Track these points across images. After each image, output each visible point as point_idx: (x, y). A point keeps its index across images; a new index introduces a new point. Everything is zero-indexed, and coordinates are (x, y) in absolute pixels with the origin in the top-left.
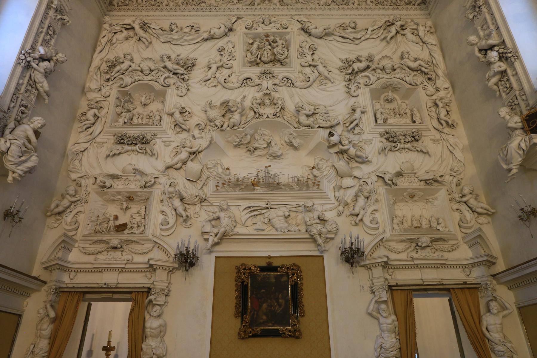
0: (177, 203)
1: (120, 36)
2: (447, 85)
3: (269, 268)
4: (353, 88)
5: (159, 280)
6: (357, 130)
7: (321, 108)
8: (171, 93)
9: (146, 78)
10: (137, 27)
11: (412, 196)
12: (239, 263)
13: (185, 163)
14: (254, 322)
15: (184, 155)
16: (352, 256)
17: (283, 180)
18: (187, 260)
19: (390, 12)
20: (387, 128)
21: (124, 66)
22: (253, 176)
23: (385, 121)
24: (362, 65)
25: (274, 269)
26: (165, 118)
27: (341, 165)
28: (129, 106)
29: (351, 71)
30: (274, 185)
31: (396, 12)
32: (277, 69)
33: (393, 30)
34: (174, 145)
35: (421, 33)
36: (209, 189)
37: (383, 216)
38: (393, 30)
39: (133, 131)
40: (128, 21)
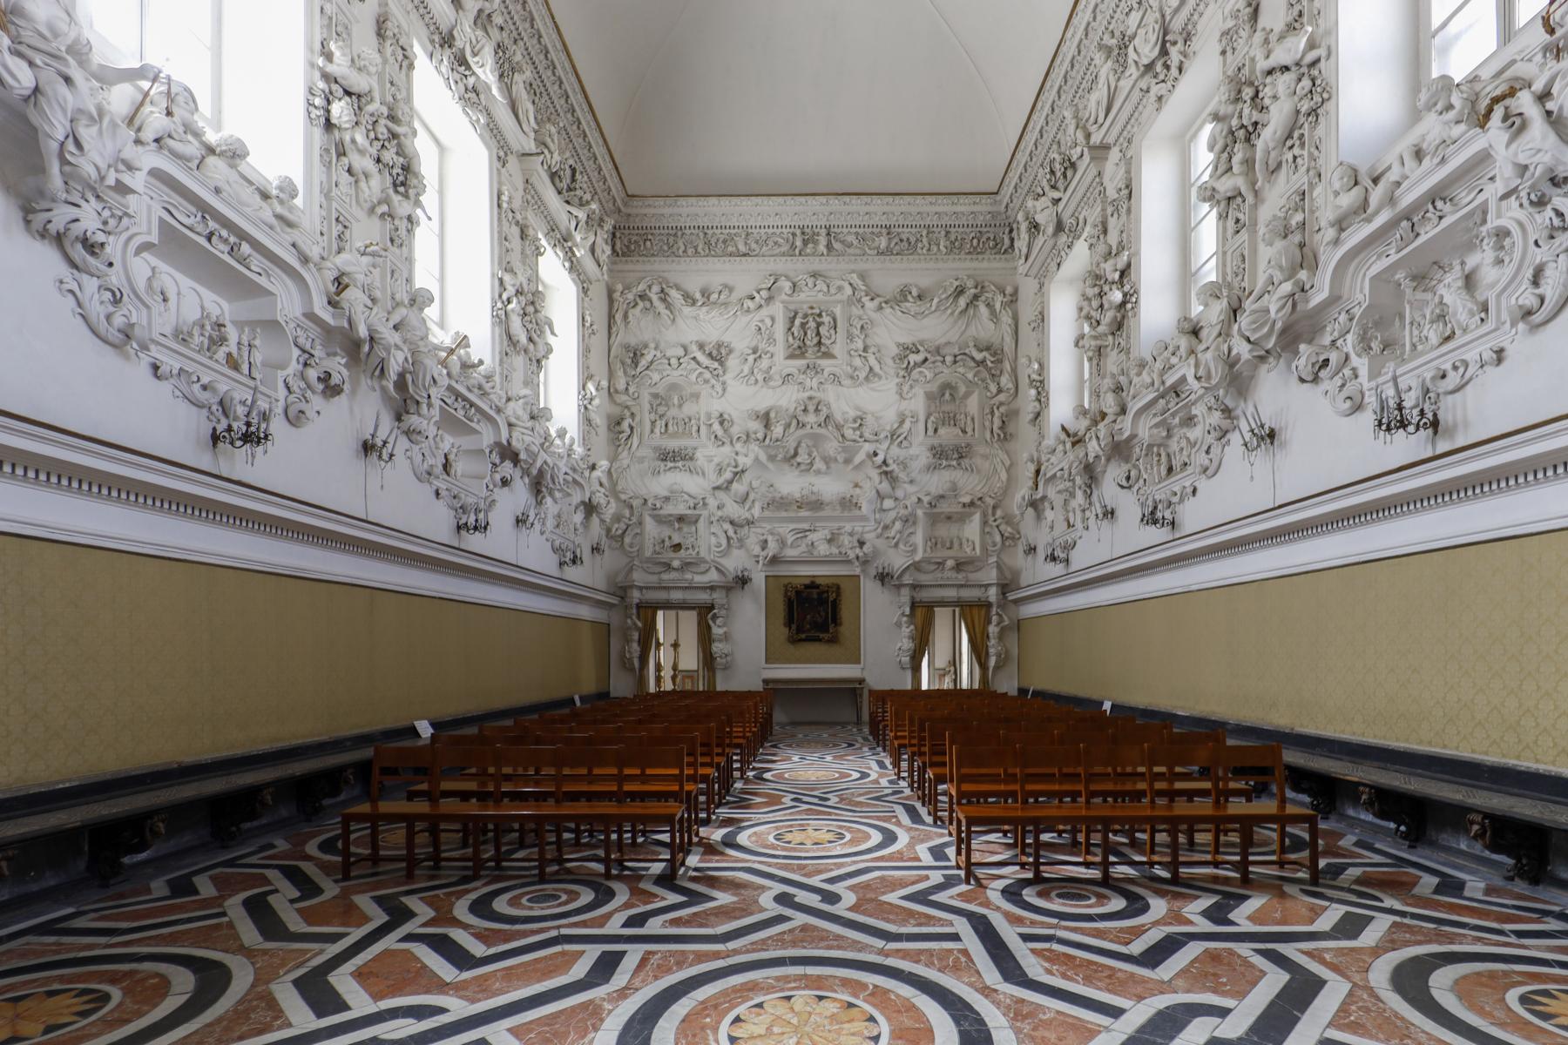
0: (727, 526)
1: (637, 311)
2: (1010, 385)
3: (812, 585)
4: (906, 388)
5: (718, 597)
6: (905, 443)
7: (869, 417)
8: (705, 391)
9: (676, 373)
10: (654, 298)
11: (949, 518)
12: (786, 581)
13: (731, 482)
14: (799, 631)
15: (728, 475)
16: (883, 577)
17: (827, 497)
18: (743, 581)
19: (968, 264)
20: (936, 442)
21: (649, 358)
22: (797, 496)
23: (936, 430)
24: (919, 358)
25: (818, 587)
26: (703, 428)
27: (885, 486)
28: (661, 410)
29: (910, 358)
30: (816, 504)
31: (975, 264)
32: (824, 363)
33: (962, 302)
34: (716, 460)
35: (998, 306)
36: (756, 511)
37: (919, 539)
38: (962, 302)
39: (672, 444)
40: (641, 287)
